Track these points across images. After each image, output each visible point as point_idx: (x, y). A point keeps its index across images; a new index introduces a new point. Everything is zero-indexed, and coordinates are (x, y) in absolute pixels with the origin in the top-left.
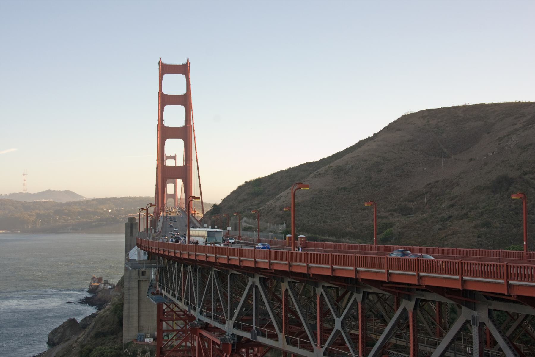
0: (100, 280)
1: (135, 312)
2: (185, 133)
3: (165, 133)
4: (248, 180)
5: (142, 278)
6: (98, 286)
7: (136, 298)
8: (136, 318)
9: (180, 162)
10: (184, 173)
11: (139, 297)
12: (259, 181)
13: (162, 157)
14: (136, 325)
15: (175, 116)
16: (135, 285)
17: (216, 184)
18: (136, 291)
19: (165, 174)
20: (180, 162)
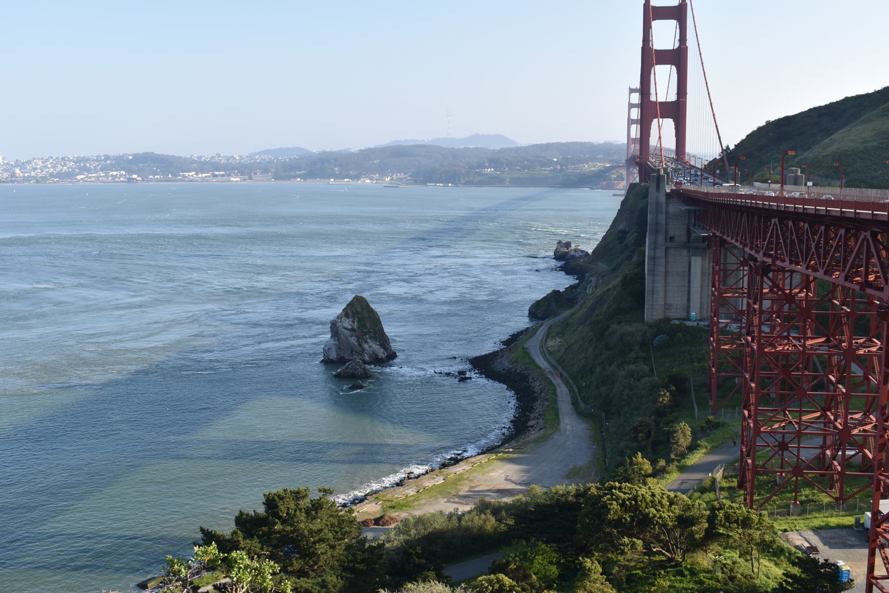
0: (568, 245)
1: (660, 286)
2: (677, 57)
3: (650, 57)
4: (772, 119)
5: (669, 244)
6: (567, 253)
7: (662, 269)
8: (661, 294)
9: (673, 98)
10: (676, 111)
11: (666, 268)
12: (787, 121)
13: (645, 88)
14: (661, 301)
15: (665, 35)
16: (661, 253)
17: (719, 123)
18: (663, 261)
19: (649, 110)
20: (673, 98)
